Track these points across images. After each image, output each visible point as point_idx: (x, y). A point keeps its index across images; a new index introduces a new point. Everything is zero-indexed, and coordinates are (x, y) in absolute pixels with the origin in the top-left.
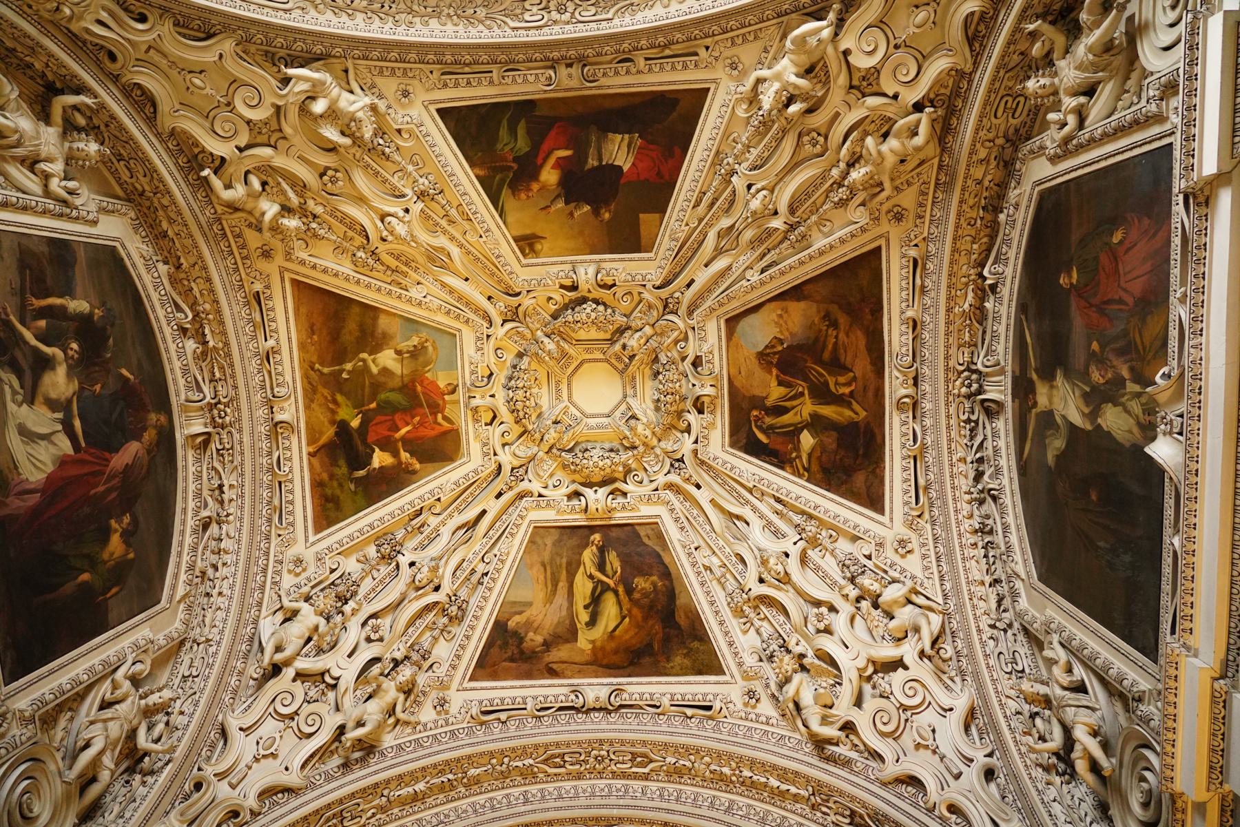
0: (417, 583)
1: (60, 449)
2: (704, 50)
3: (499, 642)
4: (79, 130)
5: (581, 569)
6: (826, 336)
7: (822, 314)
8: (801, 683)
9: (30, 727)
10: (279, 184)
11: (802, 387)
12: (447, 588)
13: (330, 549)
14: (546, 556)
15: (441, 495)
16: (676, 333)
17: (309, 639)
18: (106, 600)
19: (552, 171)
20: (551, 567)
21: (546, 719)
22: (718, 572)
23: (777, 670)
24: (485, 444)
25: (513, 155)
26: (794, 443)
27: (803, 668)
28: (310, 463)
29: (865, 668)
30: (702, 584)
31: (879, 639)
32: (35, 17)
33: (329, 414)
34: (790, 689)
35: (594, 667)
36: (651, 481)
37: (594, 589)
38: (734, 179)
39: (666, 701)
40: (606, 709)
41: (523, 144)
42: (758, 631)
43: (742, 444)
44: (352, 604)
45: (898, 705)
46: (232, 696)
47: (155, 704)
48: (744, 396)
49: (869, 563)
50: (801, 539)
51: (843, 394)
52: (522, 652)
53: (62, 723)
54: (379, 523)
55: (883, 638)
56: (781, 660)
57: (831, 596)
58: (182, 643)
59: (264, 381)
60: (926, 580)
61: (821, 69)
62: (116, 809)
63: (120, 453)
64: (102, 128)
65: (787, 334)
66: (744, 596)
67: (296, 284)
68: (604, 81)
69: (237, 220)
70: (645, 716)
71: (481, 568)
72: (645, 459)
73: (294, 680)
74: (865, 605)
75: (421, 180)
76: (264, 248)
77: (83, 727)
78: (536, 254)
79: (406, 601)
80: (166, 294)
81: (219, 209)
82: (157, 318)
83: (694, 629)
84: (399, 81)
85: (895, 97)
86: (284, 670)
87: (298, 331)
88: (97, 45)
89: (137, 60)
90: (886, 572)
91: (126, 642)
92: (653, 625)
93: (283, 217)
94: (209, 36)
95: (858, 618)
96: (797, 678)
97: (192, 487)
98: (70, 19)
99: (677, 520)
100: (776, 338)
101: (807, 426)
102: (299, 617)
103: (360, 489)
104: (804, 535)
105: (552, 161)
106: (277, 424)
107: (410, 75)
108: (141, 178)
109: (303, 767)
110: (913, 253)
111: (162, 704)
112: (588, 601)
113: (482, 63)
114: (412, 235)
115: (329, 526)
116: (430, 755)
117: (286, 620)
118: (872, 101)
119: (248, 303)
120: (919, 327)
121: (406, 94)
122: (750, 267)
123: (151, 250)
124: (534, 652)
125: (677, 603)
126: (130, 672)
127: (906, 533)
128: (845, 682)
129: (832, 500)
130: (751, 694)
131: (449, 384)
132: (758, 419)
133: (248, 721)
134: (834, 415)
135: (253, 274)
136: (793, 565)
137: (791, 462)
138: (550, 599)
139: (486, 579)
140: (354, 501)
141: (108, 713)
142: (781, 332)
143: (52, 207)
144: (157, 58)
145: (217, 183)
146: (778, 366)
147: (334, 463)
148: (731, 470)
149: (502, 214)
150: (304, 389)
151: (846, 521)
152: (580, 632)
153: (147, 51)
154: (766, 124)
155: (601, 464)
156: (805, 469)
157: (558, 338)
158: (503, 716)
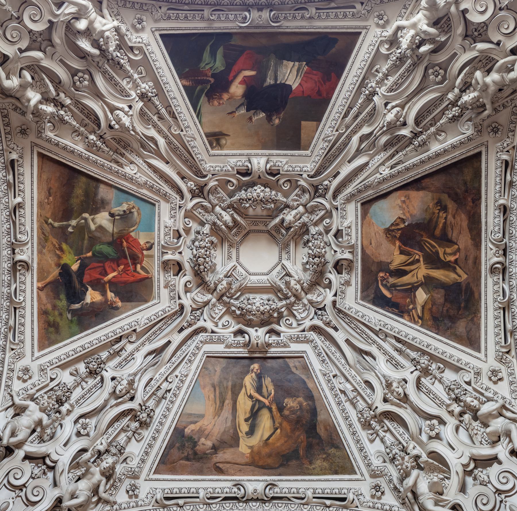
0: (118, 392)
2: (360, 5)
5: (243, 390)
7: (436, 201)
8: (418, 477)
11: (418, 255)
13: (51, 363)
14: (216, 379)
15: (137, 327)
16: (323, 212)
17: (34, 431)
19: (239, 85)
20: (220, 388)
21: (214, 505)
23: (399, 467)
25: (212, 72)
26: (411, 298)
28: (38, 296)
29: (468, 465)
31: (478, 444)
33: (56, 259)
34: (409, 482)
35: (252, 468)
36: (299, 325)
38: (376, 98)
39: (309, 493)
40: (263, 500)
41: (219, 65)
42: (382, 440)
43: (370, 298)
45: (494, 490)
48: (373, 261)
50: (417, 370)
51: (450, 261)
52: (195, 453)
55: (481, 443)
56: (403, 459)
59: (10, 229)
60: (513, 400)
65: (408, 215)
66: (372, 413)
67: (40, 155)
68: (286, 24)
72: (295, 308)
73: (23, 460)
74: (467, 417)
75: (143, 85)
76: (23, 127)
83: (331, 439)
85: (498, 44)
86: (16, 451)
87: (39, 193)
92: (299, 436)
95: (461, 428)
96: (415, 473)
99: (319, 355)
100: (400, 218)
101: (421, 285)
102: (27, 412)
103: (75, 318)
105: (240, 78)
106: (16, 262)
107: (145, 8)
110: (505, 157)
112: (248, 415)
114: (133, 126)
115: (50, 345)
117: (16, 415)
118: (481, 46)
119: (6, 168)
120: (508, 212)
122: (383, 164)
124: (205, 454)
125: (318, 418)
127: (497, 365)
128: (453, 475)
129: (441, 341)
130: (377, 488)
131: (147, 242)
132: (383, 279)
134: (442, 277)
135: (12, 146)
136: (411, 390)
137: (408, 312)
139: (169, 395)
140: (70, 328)
142: (404, 214)
146: (400, 239)
147: (57, 296)
148: (362, 317)
149: (199, 115)
151: (451, 356)
152: (241, 439)
154: (401, 59)
155: (262, 308)
156: (419, 317)
157: (233, 212)
158: (181, 502)
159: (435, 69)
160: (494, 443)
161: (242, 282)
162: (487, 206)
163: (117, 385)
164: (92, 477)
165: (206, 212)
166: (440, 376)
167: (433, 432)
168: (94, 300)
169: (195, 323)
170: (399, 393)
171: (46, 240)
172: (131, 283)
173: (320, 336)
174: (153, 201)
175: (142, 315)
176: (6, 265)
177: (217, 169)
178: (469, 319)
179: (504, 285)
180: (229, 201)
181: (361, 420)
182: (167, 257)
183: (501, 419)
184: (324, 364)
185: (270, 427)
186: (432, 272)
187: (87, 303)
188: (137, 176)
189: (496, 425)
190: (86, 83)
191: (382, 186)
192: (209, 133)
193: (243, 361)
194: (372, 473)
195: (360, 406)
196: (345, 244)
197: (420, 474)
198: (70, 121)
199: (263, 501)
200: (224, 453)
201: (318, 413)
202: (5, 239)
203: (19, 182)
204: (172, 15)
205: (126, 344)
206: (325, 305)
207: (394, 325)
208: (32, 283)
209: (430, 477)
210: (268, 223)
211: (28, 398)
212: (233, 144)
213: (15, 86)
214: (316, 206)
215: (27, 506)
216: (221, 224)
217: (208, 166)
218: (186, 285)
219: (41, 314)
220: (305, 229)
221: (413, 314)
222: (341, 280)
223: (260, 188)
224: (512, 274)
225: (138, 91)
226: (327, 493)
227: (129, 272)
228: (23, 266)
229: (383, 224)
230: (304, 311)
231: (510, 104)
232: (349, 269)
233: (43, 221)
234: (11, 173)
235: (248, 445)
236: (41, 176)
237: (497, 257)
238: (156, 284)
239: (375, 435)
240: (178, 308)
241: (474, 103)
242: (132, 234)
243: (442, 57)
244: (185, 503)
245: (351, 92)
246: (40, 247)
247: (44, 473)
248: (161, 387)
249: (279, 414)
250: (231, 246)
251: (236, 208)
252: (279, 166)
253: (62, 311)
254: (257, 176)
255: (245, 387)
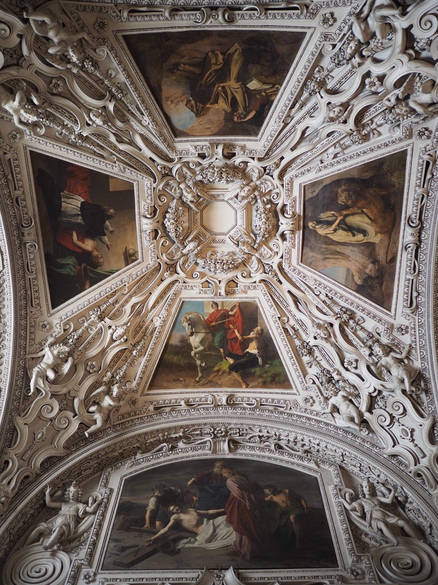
0: (326, 337)
1: (222, 522)
2: (6, 155)
3: (369, 291)
4: (64, 494)
5: (329, 236)
6: (184, 71)
7: (170, 74)
9: (362, 558)
10: (94, 396)
11: (218, 88)
12: (331, 319)
14: (319, 256)
15: (277, 316)
16: (184, 169)
17: (351, 401)
18: (307, 508)
21: (421, 268)
22: (339, 149)
23: (405, 117)
24: (249, 288)
27: (407, 97)
29: (410, 55)
30: (345, 160)
31: (391, 43)
32: (7, 513)
33: (225, 375)
34: (419, 110)
35: (393, 234)
37: (343, 229)
39: (420, 191)
41: (71, 261)
43: (256, 128)
44: (334, 375)
46: (375, 447)
47: (369, 491)
49: (339, 46)
50: (319, 92)
51: (223, 59)
52: (377, 277)
53: (367, 540)
54: (289, 353)
55: (390, 39)
57: (358, 75)
58: (341, 467)
59: (204, 408)
61: (9, 84)
62: (421, 520)
63: (231, 490)
64: (64, 482)
65: (183, 98)
66: (355, 133)
67: (150, 388)
68: (31, 214)
69: (114, 417)
70: (428, 205)
71: (323, 297)
75: (92, 319)
77: (372, 530)
78: (136, 252)
79: (336, 343)
80: (152, 455)
81: (108, 426)
82: (164, 462)
84: (37, 330)
85: (20, 36)
86: (365, 418)
87: (177, 388)
88: (21, 484)
89: (28, 465)
90: (345, 35)
91: (333, 500)
93: (112, 394)
94: (15, 429)
97: (258, 452)
98: (7, 497)
99: (303, 174)
100: (186, 105)
101: (244, 85)
102: (337, 405)
104: (317, 90)
105: (80, 244)
107: (33, 324)
108: (90, 464)
109: (422, 416)
110: (125, 14)
111: (370, 487)
112: (350, 234)
113: (25, 284)
114: (124, 325)
116: (430, 342)
117: (338, 411)
118: (25, 51)
119: (160, 413)
120: (176, 7)
121: (44, 326)
122: (140, 122)
123: (129, 461)
124: (378, 270)
125: (357, 177)
126: (348, 501)
127: (319, 18)
129: (295, 69)
131: (212, 307)
132: (239, 117)
133: (391, 443)
134: (237, 66)
135: (144, 410)
138: (346, 257)
140: (276, 366)
141: (368, 516)
142: (182, 101)
143: (101, 512)
144: (26, 457)
145: (93, 428)
146: (205, 104)
147: (253, 374)
150: (210, 387)
151: (309, 61)
152: (369, 241)
153: (24, 460)
154: (49, 116)
155: (264, 220)
156: (273, 87)
157: (187, 241)
158: (415, 294)
159: (52, 88)
160: (392, 29)
161: (242, 232)
162: (172, 27)
163: (321, 336)
164: (389, 364)
165: (187, 261)
166: (326, 71)
167: (376, 83)
168: (256, 347)
169: (275, 271)
170: (339, 111)
171: (211, 382)
172: (243, 319)
173: (288, 171)
174: (181, 303)
175: (268, 312)
176: (230, 411)
177: (153, 255)
178: (275, 41)
179: (244, 9)
180: (177, 244)
181: (360, 142)
182: (223, 292)
183: (370, 21)
184: (311, 170)
185: (361, 217)
186: (233, 75)
187: (258, 352)
188: (162, 317)
189: (375, 27)
190: (94, 363)
191: (159, 121)
192: (125, 263)
193: (306, 234)
194: (408, 137)
195: (349, 142)
196: (211, 152)
197: (414, 99)
198: (123, 371)
199: (422, 228)
200: (379, 255)
201: (352, 177)
202: (211, 412)
203: (170, 403)
204: (36, 303)
205: (289, 325)
206: (261, 167)
207: (280, 110)
208: (243, 392)
209: (417, 89)
210: (194, 212)
211: (326, 403)
212: (133, 244)
213: (100, 416)
214: (179, 175)
215: (406, 415)
216: (196, 250)
217: (151, 263)
218: (244, 277)
219: (266, 386)
220: (199, 184)
221: (270, 92)
222: (241, 154)
223: (166, 222)
224: (233, 2)
225: (97, 321)
226: (421, 175)
227: (234, 320)
228: (231, 399)
229: (192, 119)
230: (266, 184)
231: (76, 14)
232: (231, 147)
233: (198, 384)
234: (163, 408)
235: (374, 235)
236: (165, 387)
237: (218, 17)
238: (244, 300)
239: (375, 131)
240: (262, 284)
241: (79, 51)
242: (206, 318)
243: (41, 84)
244: (417, 291)
245: (81, 154)
246: (216, 386)
247: (383, 398)
248: (323, 300)
249: (351, 209)
250: (214, 241)
251: (183, 238)
252: (148, 207)
253: (263, 371)
254: (157, 224)
255: (327, 234)
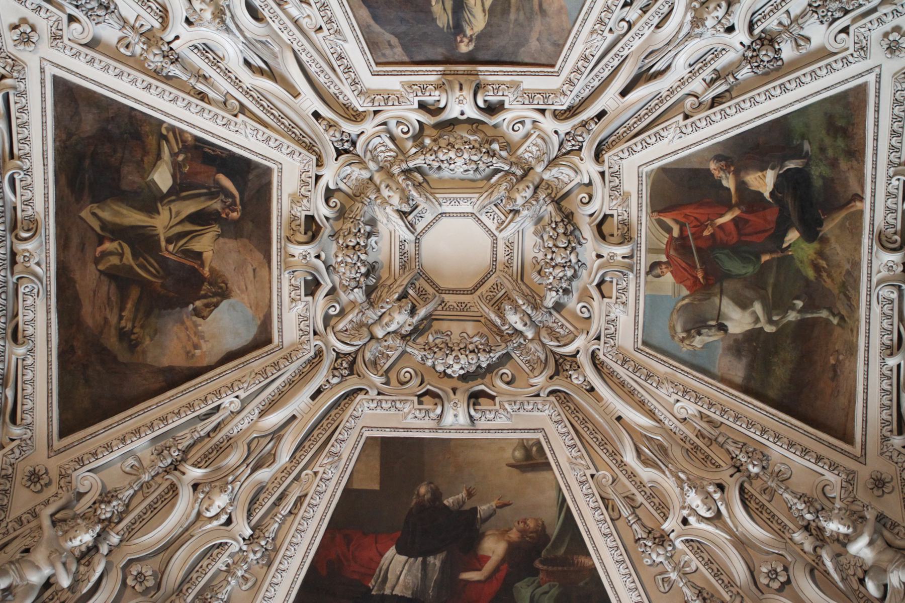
11: (169, 251)
14: (538, 25)
33: (827, 251)
78: (523, 445)
87: (854, 372)
99: (348, 69)
101: (162, 197)
105: (489, 567)
132: (232, 207)
146: (202, 279)
147: (829, 183)
156: (166, 138)
171: (844, 286)
233: (848, 320)
